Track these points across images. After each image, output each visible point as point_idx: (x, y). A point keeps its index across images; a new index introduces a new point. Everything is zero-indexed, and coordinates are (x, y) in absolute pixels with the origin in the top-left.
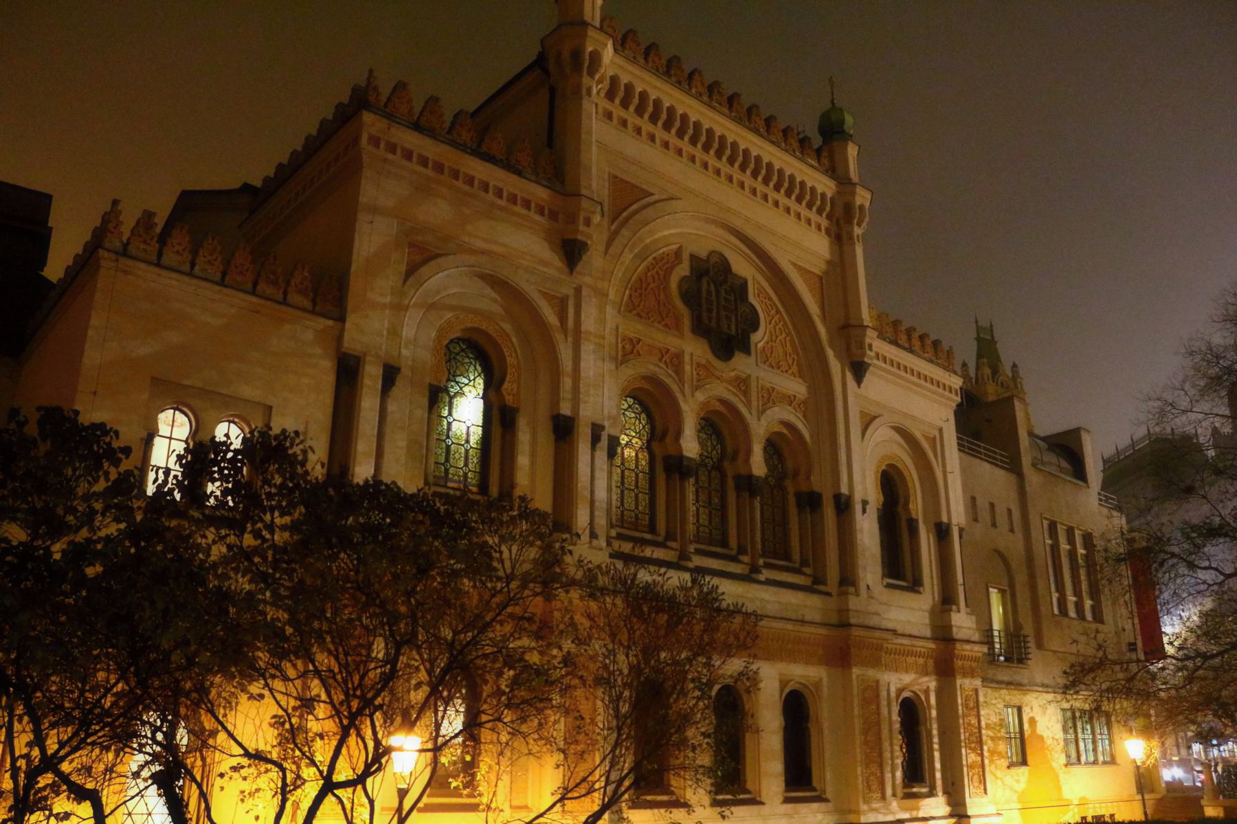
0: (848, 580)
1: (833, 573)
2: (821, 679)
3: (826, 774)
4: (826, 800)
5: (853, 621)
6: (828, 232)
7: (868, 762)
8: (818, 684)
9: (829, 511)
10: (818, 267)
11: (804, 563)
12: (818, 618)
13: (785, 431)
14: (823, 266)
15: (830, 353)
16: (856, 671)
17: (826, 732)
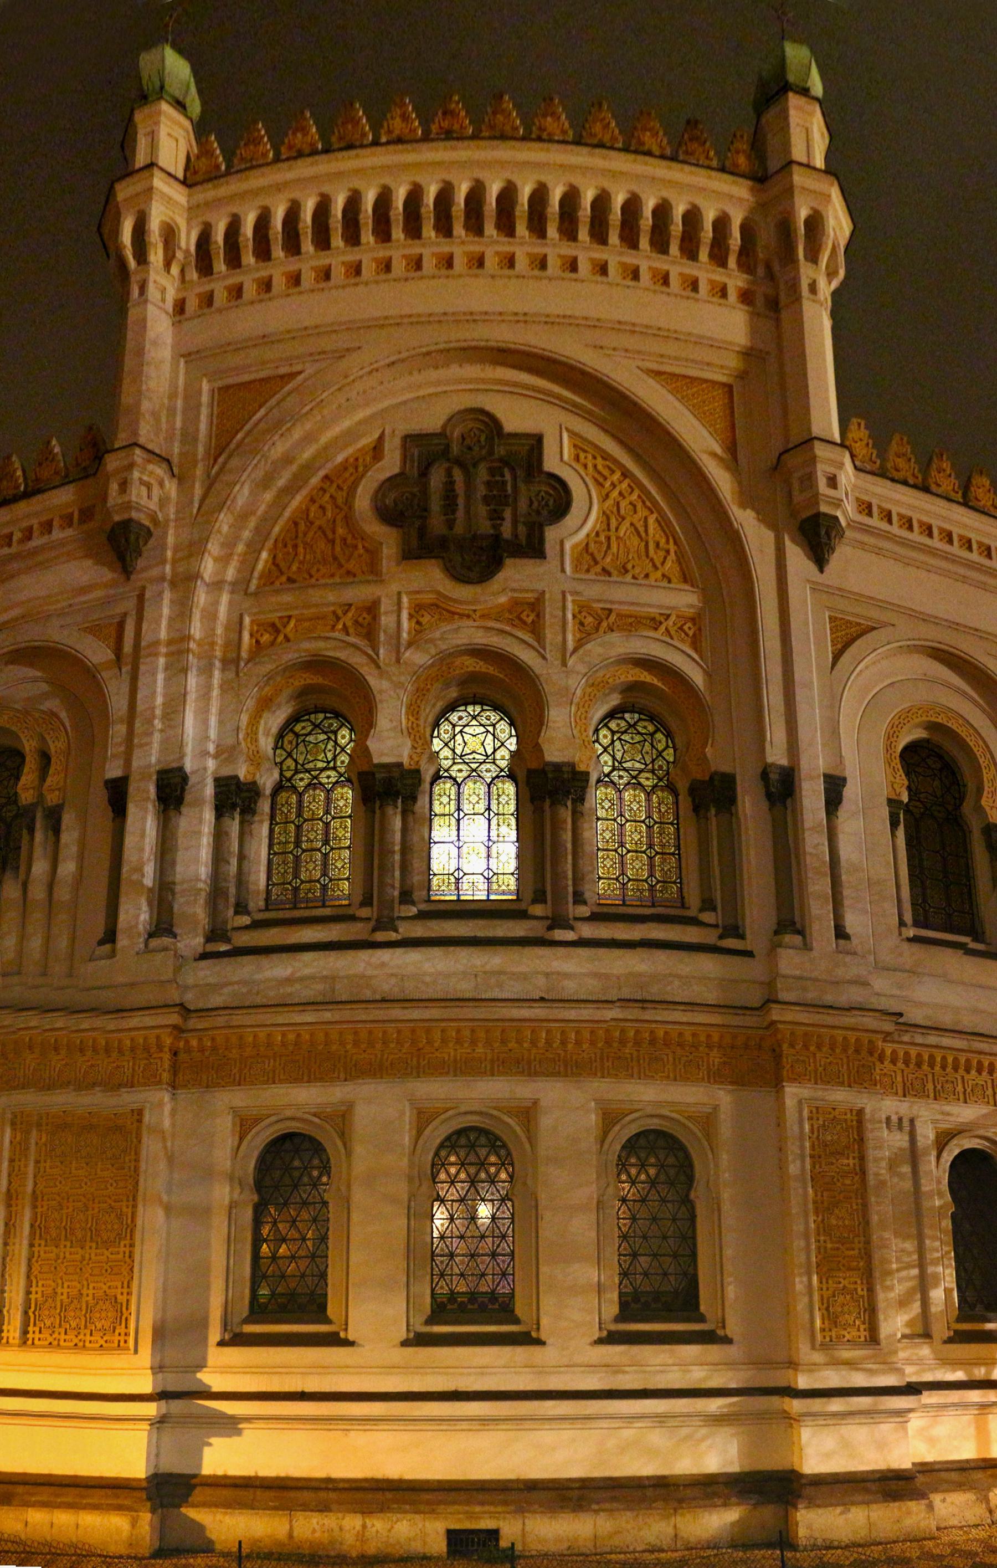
0: (790, 923)
1: (758, 911)
2: (716, 1108)
3: (728, 1292)
4: (727, 1341)
5: (783, 996)
6: (746, 297)
7: (828, 1266)
8: (708, 1121)
9: (750, 804)
10: (723, 366)
11: (708, 904)
12: (711, 997)
13: (646, 677)
14: (733, 362)
15: (746, 520)
16: (793, 1093)
17: (726, 1207)
